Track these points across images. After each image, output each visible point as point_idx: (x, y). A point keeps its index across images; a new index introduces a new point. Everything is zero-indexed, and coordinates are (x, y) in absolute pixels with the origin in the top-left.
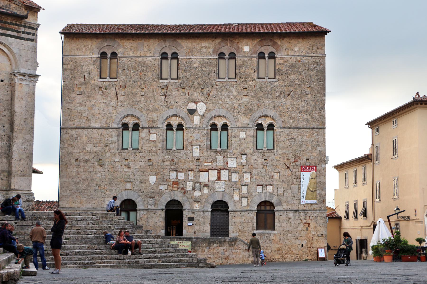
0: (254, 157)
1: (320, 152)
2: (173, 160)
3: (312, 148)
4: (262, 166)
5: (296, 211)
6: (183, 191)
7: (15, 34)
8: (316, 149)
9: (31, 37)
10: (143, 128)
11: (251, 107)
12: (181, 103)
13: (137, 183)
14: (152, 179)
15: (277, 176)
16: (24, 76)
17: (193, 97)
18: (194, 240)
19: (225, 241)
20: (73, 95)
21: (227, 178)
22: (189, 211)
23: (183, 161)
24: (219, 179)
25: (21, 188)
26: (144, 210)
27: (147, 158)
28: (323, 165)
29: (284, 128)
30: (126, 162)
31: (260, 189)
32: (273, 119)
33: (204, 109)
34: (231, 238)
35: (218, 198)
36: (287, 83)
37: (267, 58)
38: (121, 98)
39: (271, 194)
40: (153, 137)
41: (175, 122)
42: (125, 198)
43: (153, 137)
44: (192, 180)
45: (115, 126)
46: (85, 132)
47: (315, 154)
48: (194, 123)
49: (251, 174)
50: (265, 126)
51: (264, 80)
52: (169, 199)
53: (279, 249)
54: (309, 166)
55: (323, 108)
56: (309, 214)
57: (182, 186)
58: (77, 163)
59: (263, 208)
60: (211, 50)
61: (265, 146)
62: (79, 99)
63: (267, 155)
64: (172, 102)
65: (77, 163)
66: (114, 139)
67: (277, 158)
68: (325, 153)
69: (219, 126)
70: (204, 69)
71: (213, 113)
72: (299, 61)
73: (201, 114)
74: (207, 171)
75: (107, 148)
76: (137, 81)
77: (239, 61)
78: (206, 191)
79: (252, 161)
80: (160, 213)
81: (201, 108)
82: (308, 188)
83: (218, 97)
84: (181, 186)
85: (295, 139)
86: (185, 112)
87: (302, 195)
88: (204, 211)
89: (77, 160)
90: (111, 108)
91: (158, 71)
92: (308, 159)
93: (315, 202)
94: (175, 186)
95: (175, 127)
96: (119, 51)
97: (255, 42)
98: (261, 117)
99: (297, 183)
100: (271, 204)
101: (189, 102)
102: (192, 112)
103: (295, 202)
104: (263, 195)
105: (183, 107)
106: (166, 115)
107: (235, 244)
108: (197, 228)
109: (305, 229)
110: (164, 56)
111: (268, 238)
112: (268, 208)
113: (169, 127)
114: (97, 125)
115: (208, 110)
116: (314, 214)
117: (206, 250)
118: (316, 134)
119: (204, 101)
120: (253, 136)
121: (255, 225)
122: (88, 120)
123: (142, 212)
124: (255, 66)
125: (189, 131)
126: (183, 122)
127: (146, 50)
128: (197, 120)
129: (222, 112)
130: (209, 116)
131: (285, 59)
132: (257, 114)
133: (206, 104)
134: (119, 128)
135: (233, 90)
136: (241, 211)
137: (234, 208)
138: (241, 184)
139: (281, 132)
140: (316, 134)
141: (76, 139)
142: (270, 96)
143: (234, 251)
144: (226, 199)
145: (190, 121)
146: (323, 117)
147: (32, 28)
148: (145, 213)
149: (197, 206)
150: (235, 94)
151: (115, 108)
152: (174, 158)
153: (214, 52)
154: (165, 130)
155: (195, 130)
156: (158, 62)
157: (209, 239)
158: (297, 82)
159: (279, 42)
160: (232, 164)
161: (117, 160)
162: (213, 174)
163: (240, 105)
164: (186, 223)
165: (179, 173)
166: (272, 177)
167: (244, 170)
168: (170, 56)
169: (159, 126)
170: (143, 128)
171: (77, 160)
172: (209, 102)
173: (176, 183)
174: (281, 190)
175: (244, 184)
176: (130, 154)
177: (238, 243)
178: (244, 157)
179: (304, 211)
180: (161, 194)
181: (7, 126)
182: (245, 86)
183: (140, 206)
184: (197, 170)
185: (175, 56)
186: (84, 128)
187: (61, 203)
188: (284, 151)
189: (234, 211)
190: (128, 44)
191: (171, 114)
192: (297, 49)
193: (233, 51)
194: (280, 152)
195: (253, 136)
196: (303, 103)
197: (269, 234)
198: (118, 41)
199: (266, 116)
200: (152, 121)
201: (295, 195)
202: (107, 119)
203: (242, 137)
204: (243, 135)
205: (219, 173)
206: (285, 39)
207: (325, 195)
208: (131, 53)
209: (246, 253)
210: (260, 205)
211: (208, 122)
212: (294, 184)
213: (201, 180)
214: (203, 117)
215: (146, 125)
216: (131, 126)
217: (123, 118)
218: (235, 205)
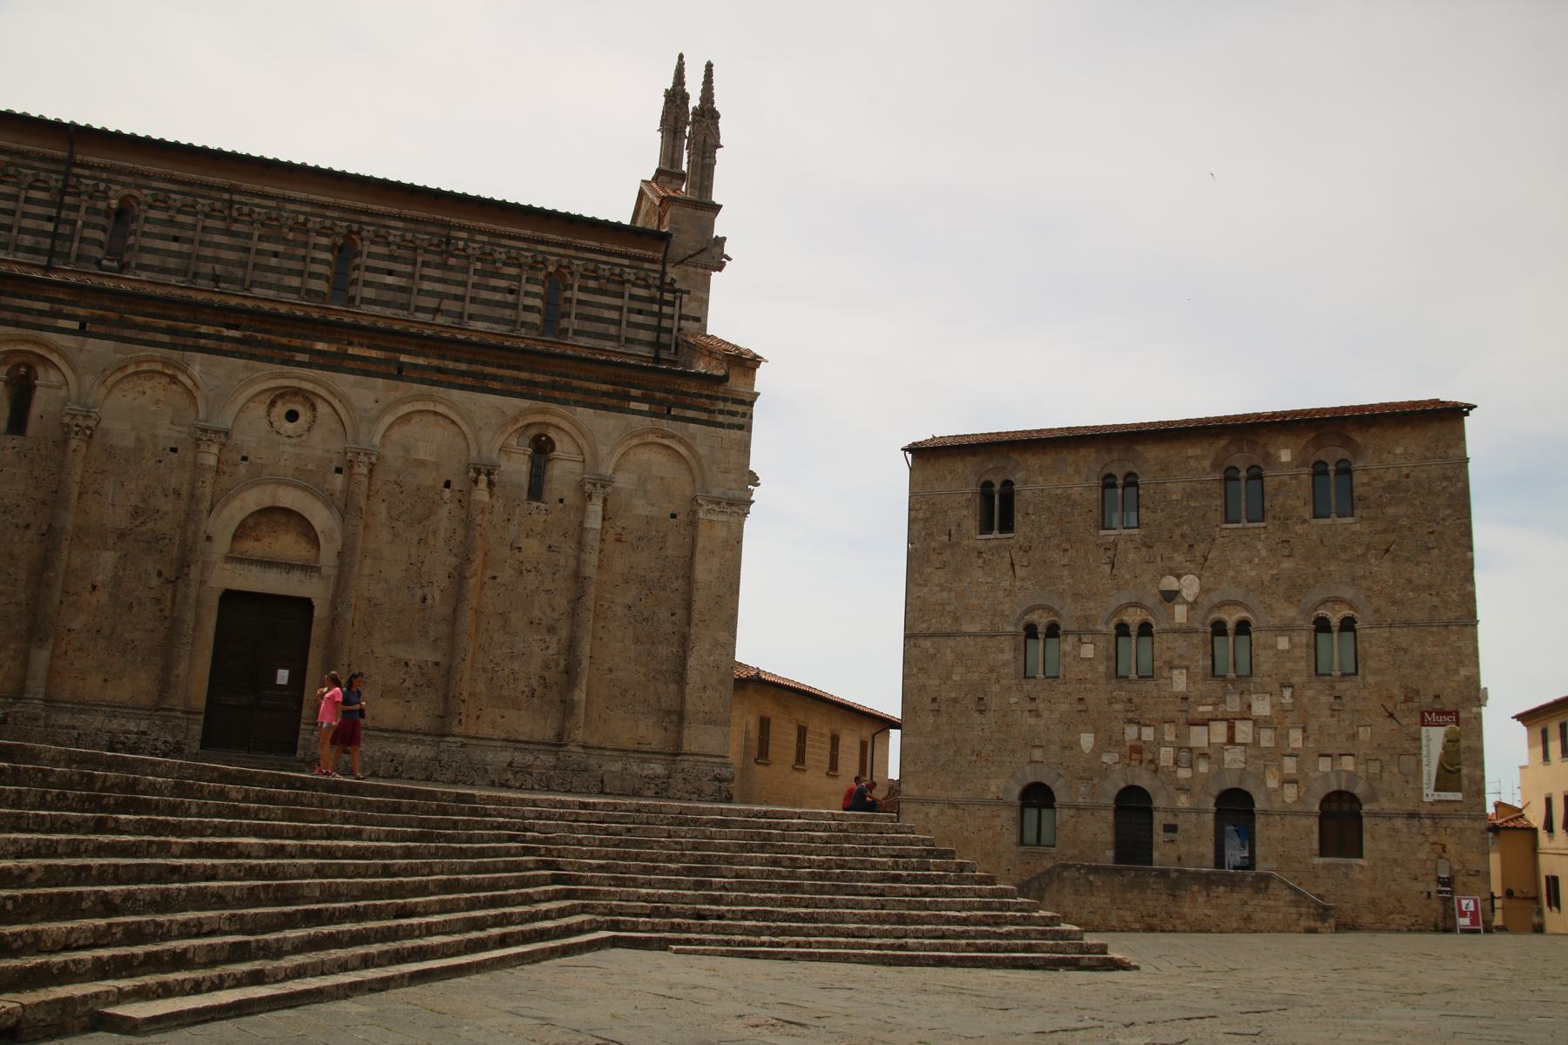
0: (1310, 693)
1: (1467, 678)
2: (1130, 700)
3: (1447, 671)
4: (1329, 713)
5: (1412, 815)
6: (1153, 767)
7: (704, 416)
8: (1456, 672)
9: (740, 421)
10: (1067, 633)
11: (1300, 581)
12: (1146, 578)
13: (1055, 748)
14: (1087, 741)
15: (1364, 734)
16: (718, 503)
18: (1173, 875)
19: (1243, 879)
20: (928, 570)
21: (1250, 740)
22: (1165, 811)
23: (1151, 701)
24: (1231, 740)
25: (705, 751)
26: (1069, 807)
27: (1076, 696)
28: (1474, 710)
29: (1379, 625)
30: (1033, 706)
31: (1324, 765)
32: (1351, 607)
33: (1196, 589)
34: (1258, 875)
35: (1231, 783)
36: (1380, 526)
37: (1332, 474)
39: (1352, 776)
40: (1088, 651)
41: (1133, 618)
42: (1031, 779)
43: (1088, 651)
44: (1171, 744)
45: (1010, 629)
46: (952, 643)
47: (1454, 685)
49: (1304, 730)
50: (1335, 621)
51: (1328, 521)
52: (1123, 785)
53: (1373, 902)
54: (1440, 713)
55: (1469, 578)
56: (1444, 823)
57: (1150, 757)
58: (935, 706)
59: (1334, 806)
60: (1207, 463)
61: (1336, 666)
62: (940, 577)
63: (1341, 686)
64: (1127, 576)
65: (935, 706)
66: (1008, 656)
67: (1365, 693)
68: (1478, 682)
69: (1231, 626)
70: (1193, 504)
71: (1216, 598)
72: (1407, 476)
73: (1190, 599)
74: (1205, 723)
75: (994, 675)
76: (1053, 536)
77: (1270, 484)
78: (1203, 767)
79: (1305, 701)
80: (1103, 813)
81: (1189, 586)
82: (1441, 766)
84: (1147, 756)
85: (1406, 651)
87: (1425, 780)
88: (1198, 812)
89: (934, 700)
90: (1000, 593)
91: (1096, 513)
92: (1437, 697)
93: (1458, 796)
94: (1135, 756)
95: (1134, 630)
96: (1017, 477)
97: (1303, 442)
98: (1324, 602)
99: (1412, 750)
100: (1353, 798)
101: (1162, 576)
102: (1170, 596)
103: (1410, 794)
104: (1333, 777)
105: (1149, 586)
106: (1113, 605)
107: (1267, 887)
108: (1183, 848)
109: (1433, 856)
110: (1108, 483)
111: (1346, 875)
112: (1346, 807)
113: (1122, 630)
114: (974, 628)
115: (1204, 591)
116: (1457, 824)
117: (1201, 899)
118: (1454, 637)
120: (1308, 646)
121: (1316, 845)
122: (956, 619)
123: (1066, 811)
124: (1306, 492)
126: (1151, 619)
127: (1070, 471)
128: (1180, 613)
129: (1236, 594)
131: (1374, 474)
132: (1316, 595)
134: (1015, 635)
135: (1260, 546)
136: (1283, 814)
137: (1266, 806)
138: (1280, 751)
139: (1370, 636)
140: (1454, 637)
141: (934, 657)
142: (1343, 556)
143: (1264, 903)
144: (1249, 787)
146: (1470, 599)
147: (742, 402)
148: (1072, 812)
149: (1183, 801)
150: (1264, 553)
151: (1008, 592)
152: (1133, 695)
153: (1215, 466)
154: (1113, 638)
156: (1097, 495)
157: (1208, 874)
158: (1405, 522)
159: (1358, 438)
160: (1261, 707)
161: (1013, 700)
162: (1219, 731)
163: (1275, 578)
164: (1159, 836)
165: (1144, 730)
166: (1355, 735)
167: (1288, 722)
168: (1120, 482)
169: (1100, 627)
170: (1067, 633)
171: (934, 700)
173: (1137, 749)
174: (1375, 768)
175: (1289, 751)
176: (1039, 688)
177: (1273, 885)
178: (1287, 693)
179: (1432, 816)
180: (1104, 772)
181: (680, 613)
182: (1285, 536)
183: (1060, 797)
184: (1182, 721)
185: (1131, 479)
186: (949, 635)
187: (904, 787)
188: (1379, 678)
189: (1266, 813)
190: (1034, 461)
191: (1123, 601)
192: (1399, 450)
193: (1257, 461)
194: (1370, 679)
195: (1308, 646)
196: (1420, 569)
197: (1349, 867)
198: (1015, 456)
199: (1337, 600)
200: (1086, 617)
201: (1410, 778)
202: (994, 615)
203: (1282, 646)
204: (1283, 643)
205: (1231, 729)
206: (1373, 430)
207: (1483, 778)
208: (1040, 479)
209: (1293, 910)
210: (1327, 799)
211: (1206, 616)
212: (1406, 753)
213: (1193, 743)
214: (1192, 606)
215: (1073, 626)
216: (1041, 629)
217: (1026, 612)
218: (1268, 800)
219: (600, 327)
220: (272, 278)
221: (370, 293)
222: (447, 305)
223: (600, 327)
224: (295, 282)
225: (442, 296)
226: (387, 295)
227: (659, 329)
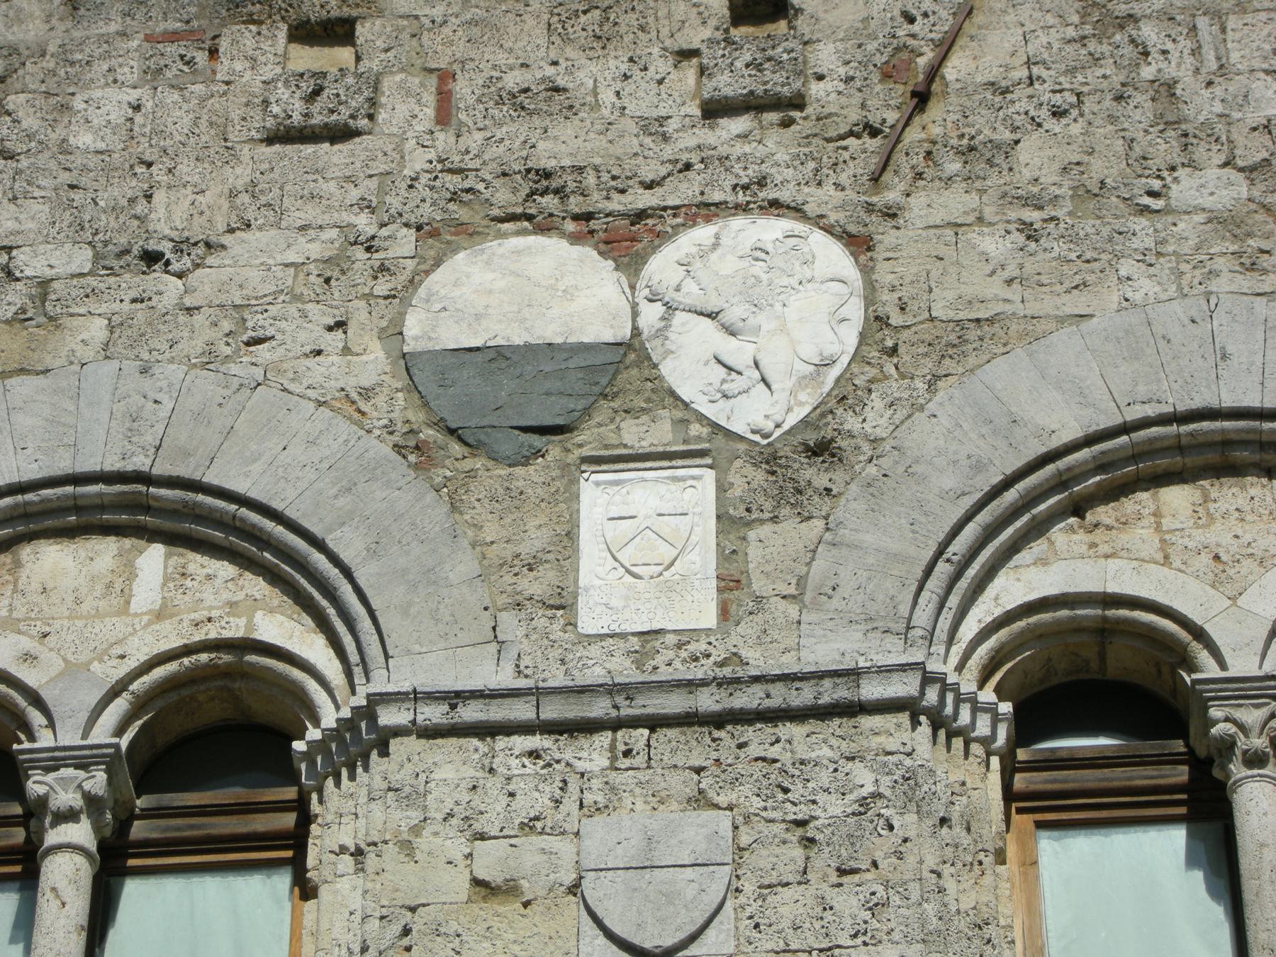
17: (560, 145)
48: (562, 604)
71: (1057, 395)
83: (1141, 111)
86: (353, 404)
105: (299, 329)
119: (822, 198)
125: (451, 765)
128: (642, 553)
130: (955, 441)
133: (858, 244)
145: (463, 565)
155: (592, 754)
172: (930, 206)
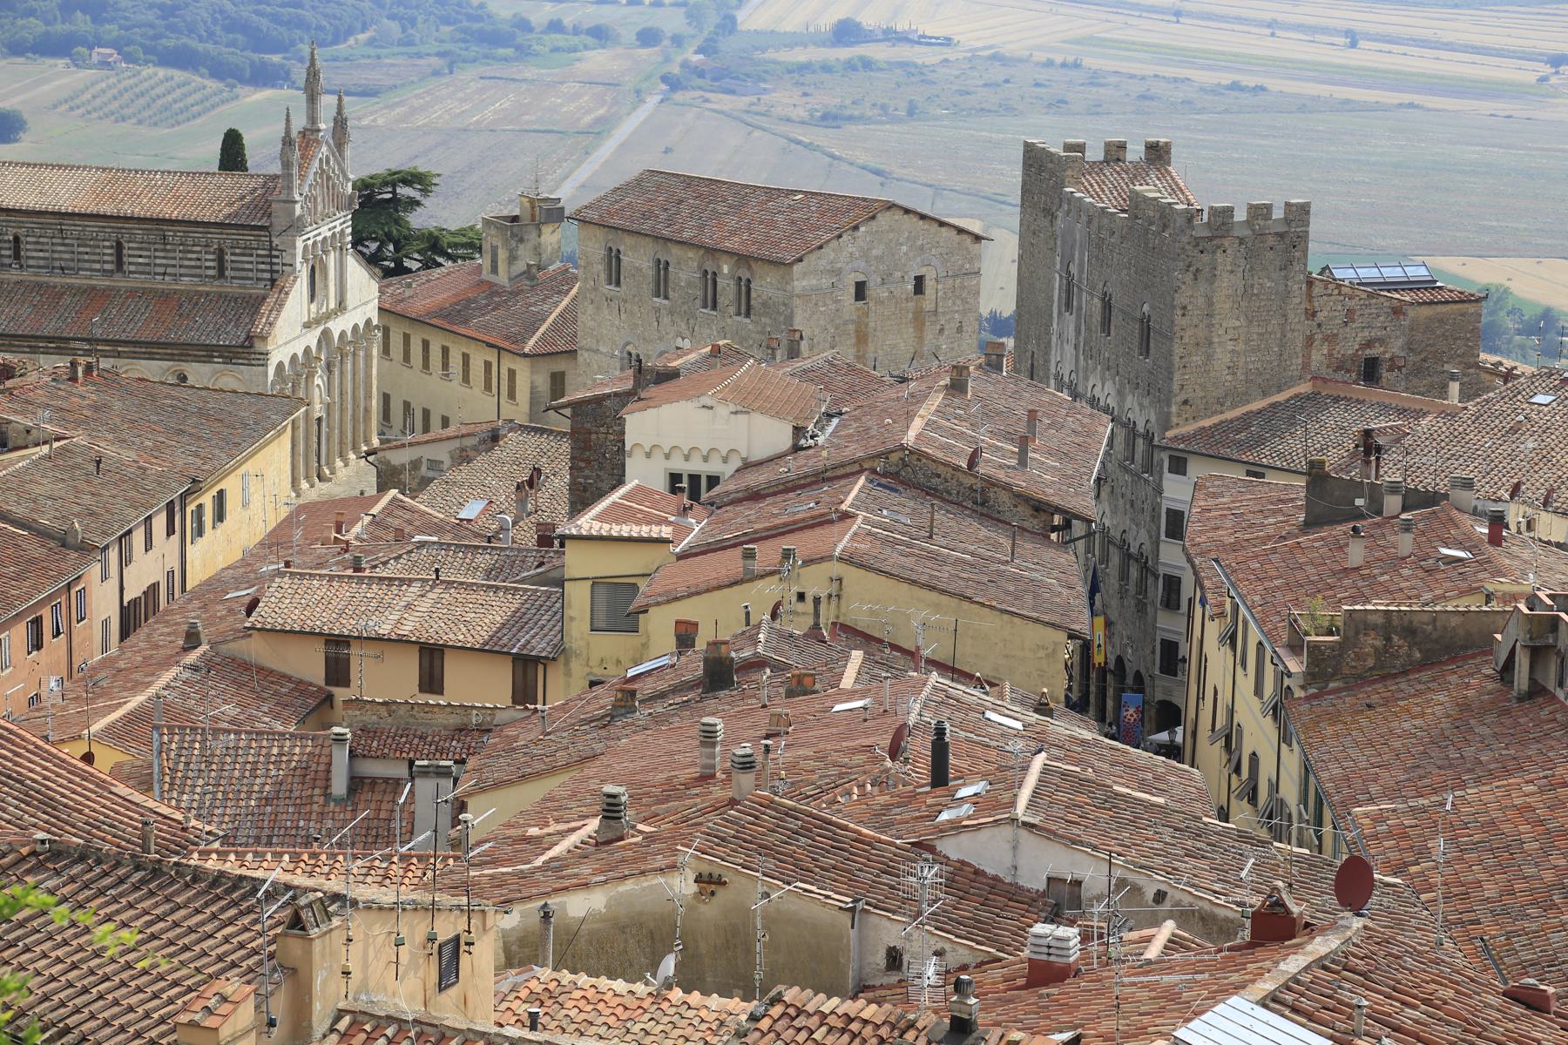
38: (623, 316)
219: (244, 274)
220: (87, 265)
221: (132, 268)
222: (169, 270)
223: (244, 274)
224: (98, 266)
225: (166, 266)
226: (141, 269)
227: (272, 271)
